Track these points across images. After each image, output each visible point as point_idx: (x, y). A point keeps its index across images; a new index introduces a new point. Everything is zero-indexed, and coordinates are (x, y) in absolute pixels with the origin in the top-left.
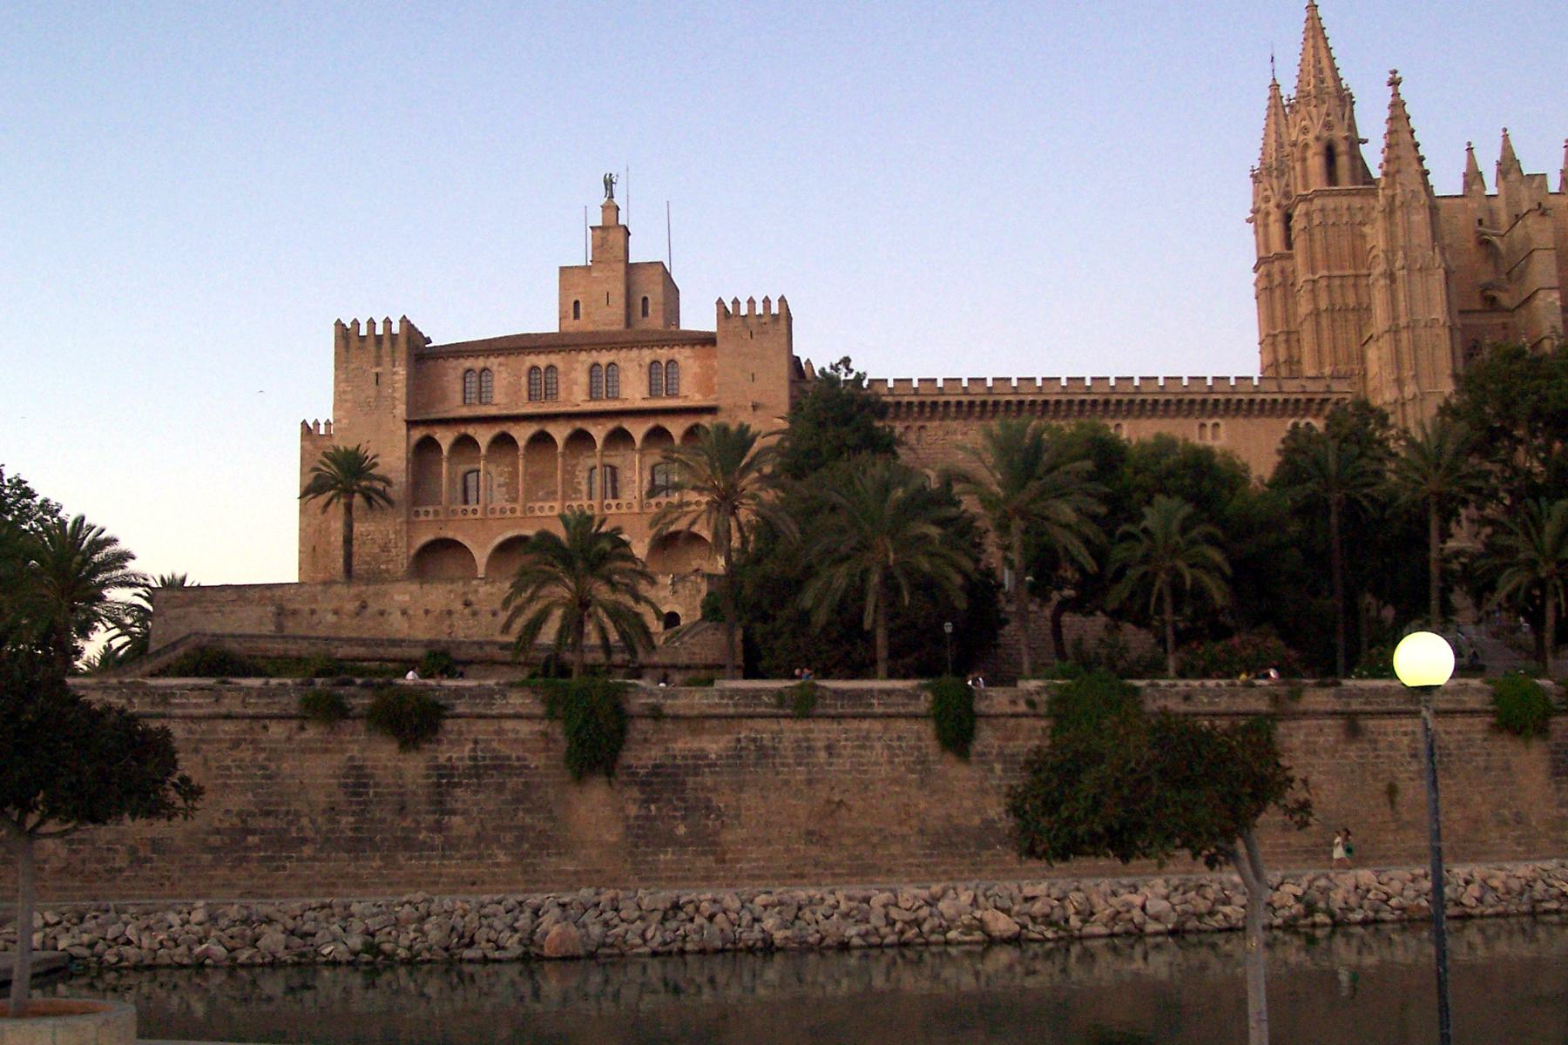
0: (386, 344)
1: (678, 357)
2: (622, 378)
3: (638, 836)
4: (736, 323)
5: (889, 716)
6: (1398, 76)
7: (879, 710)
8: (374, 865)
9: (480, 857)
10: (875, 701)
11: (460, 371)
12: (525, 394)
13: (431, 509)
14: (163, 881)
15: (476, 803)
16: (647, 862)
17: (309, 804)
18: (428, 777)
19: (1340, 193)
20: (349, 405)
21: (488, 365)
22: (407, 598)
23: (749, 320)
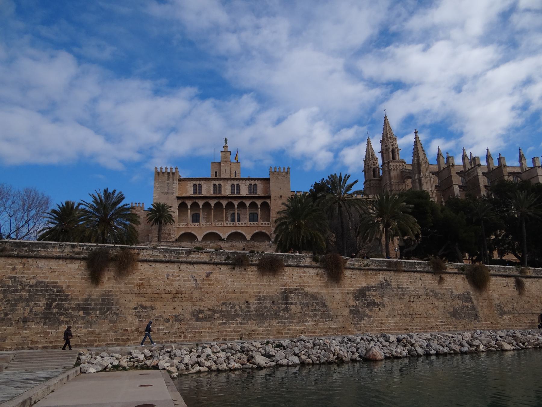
0: (171, 175)
1: (257, 183)
2: (240, 188)
6: (416, 131)
7: (418, 269)
8: (264, 325)
9: (303, 322)
10: (416, 266)
11: (192, 185)
12: (212, 192)
13: (184, 224)
15: (299, 300)
16: (359, 324)
17: (238, 300)
18: (282, 289)
19: (396, 162)
20: (158, 192)
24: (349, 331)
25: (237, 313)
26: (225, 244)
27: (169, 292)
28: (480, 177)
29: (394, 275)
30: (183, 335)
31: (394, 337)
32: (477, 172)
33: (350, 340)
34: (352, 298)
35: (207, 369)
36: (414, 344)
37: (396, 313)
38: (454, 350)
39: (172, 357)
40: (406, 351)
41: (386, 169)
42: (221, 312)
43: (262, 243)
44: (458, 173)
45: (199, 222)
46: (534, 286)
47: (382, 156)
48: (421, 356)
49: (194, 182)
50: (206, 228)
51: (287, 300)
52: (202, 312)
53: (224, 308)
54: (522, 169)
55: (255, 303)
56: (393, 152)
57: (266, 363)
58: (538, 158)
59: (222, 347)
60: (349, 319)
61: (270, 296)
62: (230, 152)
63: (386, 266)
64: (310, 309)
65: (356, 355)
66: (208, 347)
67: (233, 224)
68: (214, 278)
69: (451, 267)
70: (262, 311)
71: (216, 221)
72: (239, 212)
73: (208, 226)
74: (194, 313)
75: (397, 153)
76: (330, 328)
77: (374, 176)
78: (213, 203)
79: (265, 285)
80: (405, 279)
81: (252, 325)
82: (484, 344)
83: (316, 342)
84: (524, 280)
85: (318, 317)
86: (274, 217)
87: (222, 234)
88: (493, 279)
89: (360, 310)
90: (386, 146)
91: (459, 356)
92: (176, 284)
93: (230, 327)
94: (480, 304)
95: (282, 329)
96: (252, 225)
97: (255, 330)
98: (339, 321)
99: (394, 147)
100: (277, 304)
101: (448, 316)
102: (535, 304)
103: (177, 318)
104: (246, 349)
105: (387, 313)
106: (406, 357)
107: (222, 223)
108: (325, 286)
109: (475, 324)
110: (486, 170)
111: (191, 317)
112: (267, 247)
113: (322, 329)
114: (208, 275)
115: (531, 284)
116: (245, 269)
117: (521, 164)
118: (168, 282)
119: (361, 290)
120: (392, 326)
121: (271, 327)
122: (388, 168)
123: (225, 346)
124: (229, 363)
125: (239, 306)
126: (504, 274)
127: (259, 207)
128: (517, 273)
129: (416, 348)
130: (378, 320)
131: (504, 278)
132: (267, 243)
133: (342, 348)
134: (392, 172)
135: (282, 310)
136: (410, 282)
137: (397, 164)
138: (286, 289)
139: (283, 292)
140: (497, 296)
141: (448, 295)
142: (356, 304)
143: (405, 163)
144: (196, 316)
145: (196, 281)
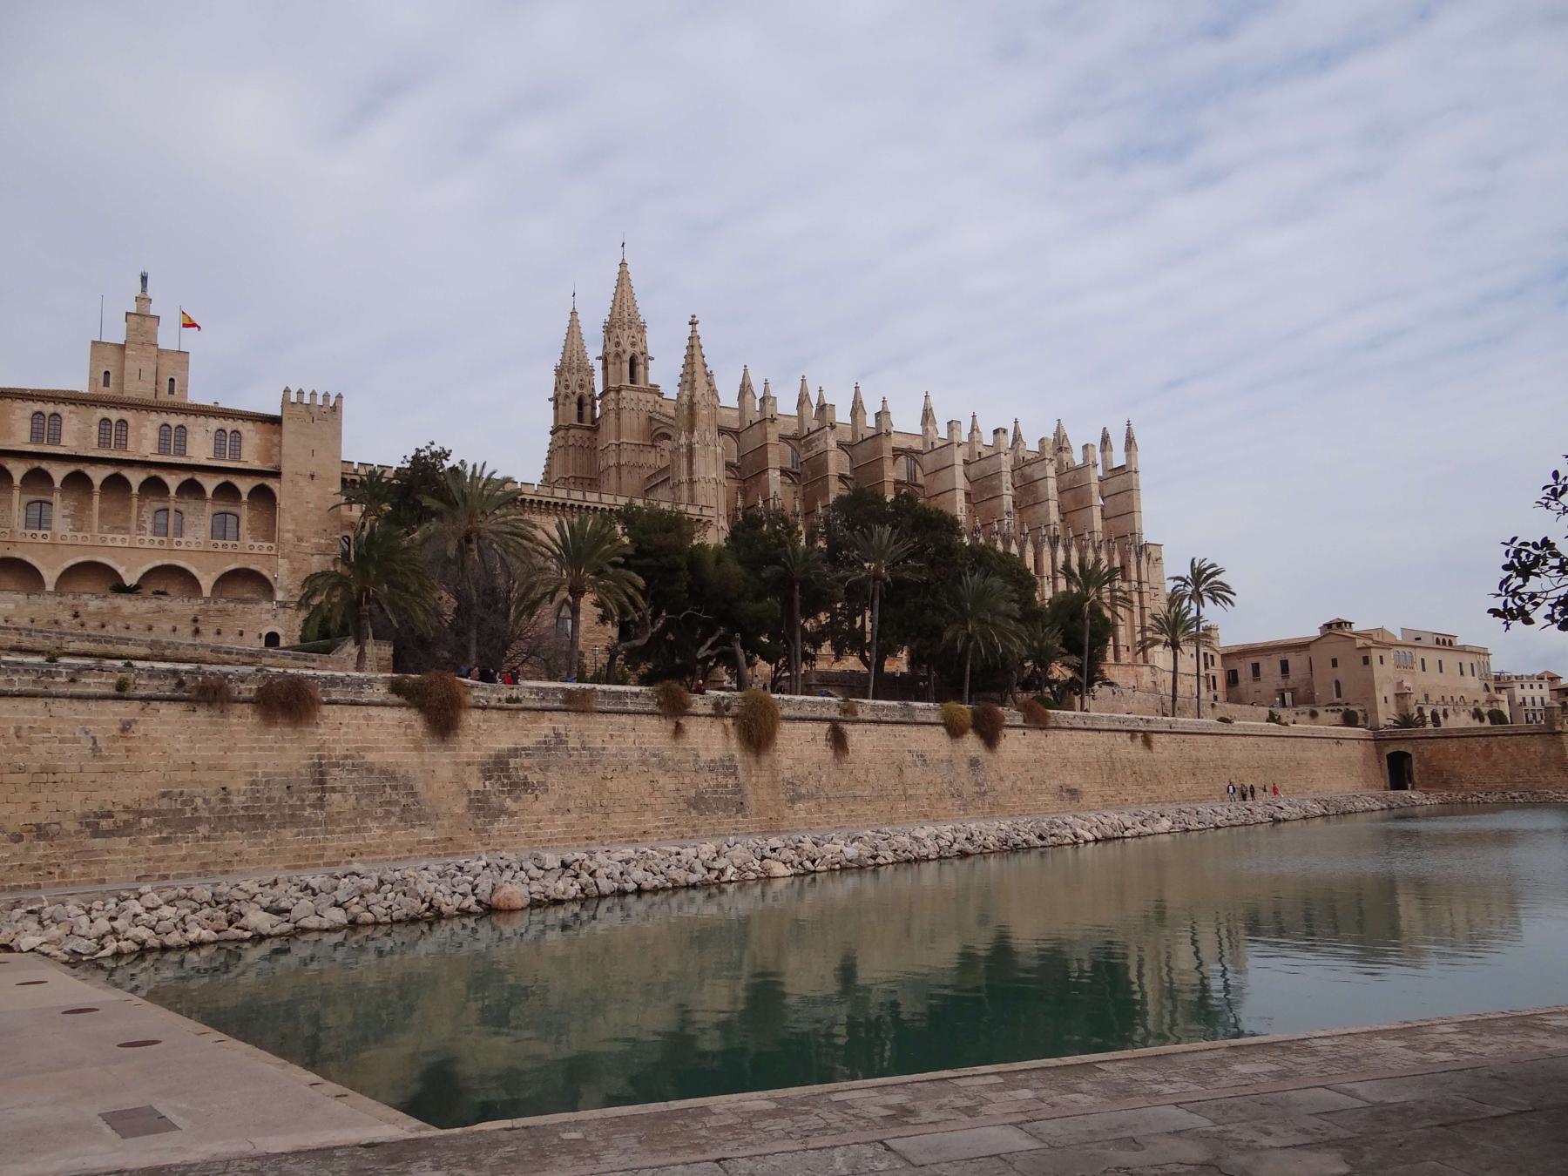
1: (240, 429)
3: (480, 809)
4: (299, 408)
5: (638, 713)
7: (630, 707)
8: (264, 841)
9: (357, 830)
10: (629, 701)
11: (29, 413)
12: (96, 441)
14: (52, 869)
15: (352, 781)
16: (486, 831)
17: (203, 786)
19: (638, 390)
21: (58, 411)
22: (11, 606)
23: (312, 408)
24: (464, 847)
25: (196, 815)
26: (138, 604)
27: (21, 770)
28: (831, 455)
29: (576, 721)
30: (57, 871)
31: (557, 860)
32: (826, 443)
33: (460, 869)
34: (477, 774)
35: (136, 948)
36: (595, 871)
37: (571, 805)
38: (675, 881)
39: (45, 923)
40: (577, 886)
41: (612, 406)
42: (158, 813)
43: (250, 606)
44: (783, 438)
45: (49, 529)
46: (866, 739)
47: (605, 368)
48: (606, 896)
49: (38, 406)
50: (74, 548)
51: (322, 782)
52: (109, 815)
53: (165, 804)
54: (925, 444)
55: (245, 791)
56: (633, 362)
57: (272, 927)
58: (960, 422)
59: (165, 895)
60: (466, 821)
61: (281, 774)
62: (159, 317)
63: (562, 701)
64: (378, 800)
65: (470, 902)
66: (132, 897)
67: (161, 543)
68: (142, 732)
69: (700, 703)
70: (260, 808)
71: (105, 527)
72: (182, 507)
73: (80, 542)
74: (88, 817)
75: (641, 368)
76: (419, 842)
77: (580, 417)
78: (98, 475)
79: (271, 749)
80: (598, 730)
81: (235, 841)
82: (737, 865)
83: (385, 877)
84: (848, 728)
85: (394, 819)
86: (288, 531)
87: (124, 568)
88: (785, 727)
89: (493, 799)
90: (618, 344)
91: (682, 894)
92: (40, 749)
93: (181, 847)
94: (754, 779)
95: (307, 849)
96: (220, 549)
97: (241, 852)
98: (442, 826)
99: (637, 350)
100: (298, 792)
101: (683, 806)
102: (864, 778)
103: (40, 832)
104: (225, 898)
105: (552, 805)
106: (574, 900)
107: (127, 537)
108: (415, 749)
109: (737, 822)
110: (848, 438)
111: (79, 828)
112: (264, 617)
113: (401, 845)
114: (126, 727)
115: (863, 735)
116: (222, 712)
117: (926, 431)
118: (20, 745)
119: (497, 756)
120: (559, 833)
121: (281, 845)
122: (618, 404)
123: (171, 894)
124: (185, 931)
125: (204, 799)
126: (812, 715)
127: (245, 498)
128: (835, 714)
129: (598, 881)
130: (532, 822)
131: (810, 725)
132: (266, 605)
133: (442, 887)
134: (625, 415)
135: (311, 806)
136: (611, 736)
137: (641, 396)
138: (321, 757)
139: (314, 763)
140: (790, 762)
141: (688, 762)
142: (485, 787)
143: (660, 395)
144: (93, 825)
145: (95, 743)
